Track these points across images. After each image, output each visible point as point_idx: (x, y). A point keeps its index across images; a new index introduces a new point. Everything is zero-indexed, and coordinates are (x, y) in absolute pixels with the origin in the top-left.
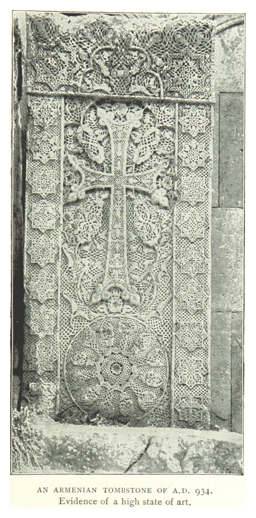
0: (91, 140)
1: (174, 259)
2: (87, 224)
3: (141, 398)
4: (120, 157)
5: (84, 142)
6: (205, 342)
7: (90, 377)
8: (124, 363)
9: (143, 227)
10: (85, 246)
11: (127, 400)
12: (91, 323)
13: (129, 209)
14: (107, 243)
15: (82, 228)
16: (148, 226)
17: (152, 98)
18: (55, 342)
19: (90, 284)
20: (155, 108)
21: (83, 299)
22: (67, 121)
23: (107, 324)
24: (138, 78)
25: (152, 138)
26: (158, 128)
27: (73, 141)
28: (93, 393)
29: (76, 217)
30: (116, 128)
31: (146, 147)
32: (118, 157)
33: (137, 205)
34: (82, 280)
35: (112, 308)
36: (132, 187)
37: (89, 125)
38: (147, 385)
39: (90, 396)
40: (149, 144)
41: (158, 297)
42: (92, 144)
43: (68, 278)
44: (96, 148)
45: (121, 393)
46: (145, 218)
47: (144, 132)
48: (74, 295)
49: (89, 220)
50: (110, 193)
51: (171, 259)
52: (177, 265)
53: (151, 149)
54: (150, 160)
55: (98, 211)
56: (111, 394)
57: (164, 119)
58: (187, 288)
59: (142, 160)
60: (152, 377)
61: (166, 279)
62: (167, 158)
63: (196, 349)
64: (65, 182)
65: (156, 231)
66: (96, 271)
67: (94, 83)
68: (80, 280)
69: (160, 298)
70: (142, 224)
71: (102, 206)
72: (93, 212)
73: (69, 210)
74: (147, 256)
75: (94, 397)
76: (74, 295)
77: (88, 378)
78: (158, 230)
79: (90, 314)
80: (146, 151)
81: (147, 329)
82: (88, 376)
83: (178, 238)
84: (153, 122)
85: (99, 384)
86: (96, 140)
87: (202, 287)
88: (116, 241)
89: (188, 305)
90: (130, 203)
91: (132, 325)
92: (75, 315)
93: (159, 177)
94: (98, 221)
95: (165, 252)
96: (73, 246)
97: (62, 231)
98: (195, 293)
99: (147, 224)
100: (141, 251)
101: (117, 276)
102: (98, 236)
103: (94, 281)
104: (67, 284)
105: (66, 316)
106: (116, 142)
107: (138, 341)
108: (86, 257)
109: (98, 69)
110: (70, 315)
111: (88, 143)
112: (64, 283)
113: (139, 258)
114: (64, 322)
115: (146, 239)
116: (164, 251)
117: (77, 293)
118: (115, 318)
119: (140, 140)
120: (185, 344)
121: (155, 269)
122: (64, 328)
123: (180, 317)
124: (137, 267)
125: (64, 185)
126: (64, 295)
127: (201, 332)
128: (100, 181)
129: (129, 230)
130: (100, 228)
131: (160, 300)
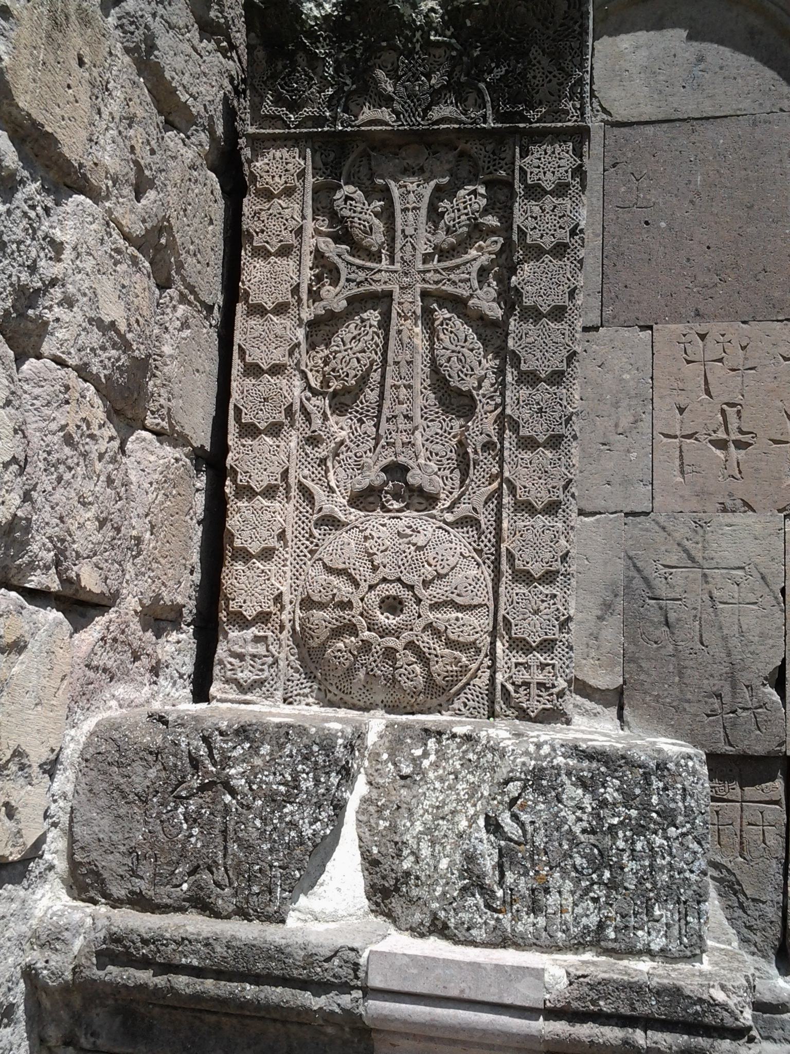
1: (508, 411)
4: (411, 237)
5: (346, 213)
9: (450, 358)
11: (409, 665)
12: (349, 527)
15: (339, 362)
17: (470, 126)
21: (338, 487)
25: (470, 200)
33: (441, 319)
42: (360, 216)
50: (392, 300)
53: (469, 219)
54: (468, 242)
57: (494, 165)
60: (458, 624)
71: (376, 323)
72: (359, 334)
77: (338, 624)
80: (459, 223)
81: (452, 537)
82: (337, 620)
85: (357, 636)
88: (400, 383)
92: (321, 514)
97: (303, 368)
98: (546, 472)
99: (459, 352)
101: (399, 444)
104: (309, 459)
107: (434, 558)
109: (372, 85)
111: (353, 215)
115: (457, 378)
122: (300, 536)
124: (439, 431)
128: (374, 281)
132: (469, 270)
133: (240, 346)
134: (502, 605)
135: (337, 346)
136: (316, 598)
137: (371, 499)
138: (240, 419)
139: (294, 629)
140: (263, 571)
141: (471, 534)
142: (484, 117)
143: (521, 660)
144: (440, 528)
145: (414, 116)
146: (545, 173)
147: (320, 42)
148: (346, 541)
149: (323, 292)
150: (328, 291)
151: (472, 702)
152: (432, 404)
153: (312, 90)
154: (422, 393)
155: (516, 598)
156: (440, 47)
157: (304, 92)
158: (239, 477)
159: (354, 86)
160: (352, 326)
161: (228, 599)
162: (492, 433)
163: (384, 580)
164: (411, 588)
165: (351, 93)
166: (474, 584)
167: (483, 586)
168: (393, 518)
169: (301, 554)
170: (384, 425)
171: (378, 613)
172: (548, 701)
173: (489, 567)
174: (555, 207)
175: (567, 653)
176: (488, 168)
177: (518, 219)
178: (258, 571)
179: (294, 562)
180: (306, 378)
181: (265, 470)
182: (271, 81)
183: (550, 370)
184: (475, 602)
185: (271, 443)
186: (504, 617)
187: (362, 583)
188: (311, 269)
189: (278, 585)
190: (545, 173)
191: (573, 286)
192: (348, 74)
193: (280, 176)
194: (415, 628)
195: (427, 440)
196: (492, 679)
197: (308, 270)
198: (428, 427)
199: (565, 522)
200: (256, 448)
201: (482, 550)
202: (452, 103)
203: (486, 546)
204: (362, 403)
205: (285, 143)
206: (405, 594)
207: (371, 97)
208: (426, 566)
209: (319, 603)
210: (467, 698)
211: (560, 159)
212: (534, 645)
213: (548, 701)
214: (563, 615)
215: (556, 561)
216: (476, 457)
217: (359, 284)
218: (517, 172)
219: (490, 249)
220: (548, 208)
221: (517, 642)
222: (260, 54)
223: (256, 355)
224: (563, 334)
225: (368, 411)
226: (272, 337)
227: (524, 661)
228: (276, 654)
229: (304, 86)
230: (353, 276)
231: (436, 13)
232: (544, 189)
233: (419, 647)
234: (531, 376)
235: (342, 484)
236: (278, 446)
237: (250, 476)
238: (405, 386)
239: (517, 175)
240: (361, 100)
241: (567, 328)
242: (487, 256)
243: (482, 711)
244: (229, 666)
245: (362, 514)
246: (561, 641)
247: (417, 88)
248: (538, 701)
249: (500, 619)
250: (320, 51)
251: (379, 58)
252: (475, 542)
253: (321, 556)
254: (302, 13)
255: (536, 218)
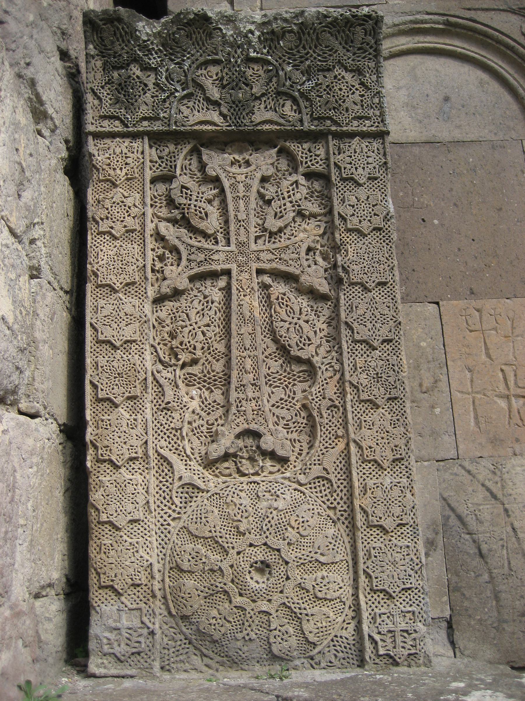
0: (194, 197)
1: (347, 377)
2: (194, 329)
3: (308, 620)
5: (183, 201)
6: (412, 514)
7: (213, 590)
8: (273, 560)
9: (288, 329)
10: (191, 366)
13: (263, 303)
14: (230, 359)
15: (186, 336)
16: (297, 326)
17: (289, 128)
18: (146, 532)
19: (204, 429)
20: (294, 146)
21: (193, 454)
22: (155, 172)
23: (238, 495)
24: (265, 101)
25: (293, 190)
26: (302, 175)
27: (165, 202)
28: (220, 619)
29: (174, 320)
30: (235, 178)
31: (285, 205)
32: (240, 221)
33: (277, 294)
34: (190, 423)
35: (245, 467)
36: (267, 266)
37: (190, 177)
38: (316, 597)
39: (215, 625)
40: (290, 199)
41: (324, 442)
43: (165, 420)
44: (204, 209)
45: (271, 615)
46: (292, 315)
47: (280, 183)
48: (176, 449)
49: (196, 323)
50: (230, 277)
51: (340, 379)
52: (353, 388)
53: (293, 206)
54: (293, 225)
55: (211, 308)
56: (254, 617)
57: (311, 161)
58: (373, 424)
59: (280, 223)
60: (325, 582)
61: (334, 412)
62: (319, 221)
63: (398, 526)
64: (154, 265)
65: (311, 335)
66: (213, 407)
67: (196, 113)
68: (186, 424)
69: (326, 445)
70: (286, 325)
71: (217, 299)
72: (203, 310)
73: (161, 310)
74: (299, 377)
75: (222, 626)
76: (176, 449)
78: (315, 332)
79: (206, 479)
80: (285, 209)
81: (308, 498)
82: (209, 589)
83: (350, 342)
84: (293, 168)
85: (230, 602)
86: (202, 198)
87: (398, 420)
88: (245, 354)
89: (377, 452)
90: (265, 294)
91: (282, 493)
92: (181, 483)
93: (309, 250)
94: (212, 323)
95: (330, 367)
96: (171, 366)
97: (152, 342)
98: (388, 432)
99: (296, 324)
100: (288, 369)
102: (214, 348)
103: (210, 422)
104: (165, 430)
105: (164, 485)
106: (236, 199)
107: (296, 520)
108: (194, 385)
110: (171, 484)
111: (189, 202)
112: (158, 429)
113: (285, 381)
114: (160, 496)
115: (296, 348)
116: (327, 366)
117: (181, 445)
118: (251, 483)
119: (274, 195)
120: (378, 519)
121: (314, 397)
122: (162, 506)
123: (364, 474)
124: (283, 396)
125: (153, 271)
126: (159, 449)
127: (405, 496)
129: (265, 337)
130: (215, 335)
131: (327, 448)
132: (298, 250)
133: (91, 325)
134: (361, 561)
135: (184, 321)
136: (185, 566)
137: (226, 464)
138: (97, 394)
139: (165, 597)
140: (130, 543)
141: (324, 493)
142: (301, 121)
143: (383, 610)
144: (295, 490)
145: (239, 118)
146: (356, 168)
147: (152, 55)
148: (209, 508)
149: (167, 273)
150: (171, 271)
151: (341, 654)
152: (275, 371)
153: (147, 95)
154: (264, 361)
155: (373, 552)
156: (257, 62)
157: (140, 96)
158: (100, 451)
159: (185, 92)
160: (196, 302)
161: (98, 574)
162: (334, 397)
163: (251, 545)
164: (279, 550)
165: (183, 98)
166: (333, 541)
167: (341, 543)
168: (251, 483)
169: (165, 523)
170: (234, 395)
171: (248, 577)
172: (411, 645)
173: (343, 523)
174: (368, 197)
175: (423, 599)
176: (306, 163)
177: (338, 208)
178: (127, 544)
179: (158, 531)
180: (156, 351)
181: (125, 443)
182: (109, 86)
183: (381, 339)
184: (337, 560)
185: (129, 417)
186: (364, 570)
187: (231, 551)
188: (153, 250)
189: (146, 557)
190: (356, 168)
191: (392, 265)
192: (178, 82)
193: (121, 169)
194: (285, 591)
195: (273, 406)
196: (358, 629)
197: (151, 252)
198: (273, 393)
199: (408, 477)
200: (114, 422)
201: (335, 508)
202: (271, 108)
203: (338, 503)
204: (209, 373)
205: (123, 140)
206: (271, 558)
207: (199, 101)
208: (290, 529)
209: (189, 572)
210: (335, 650)
211: (368, 157)
212: (394, 595)
213: (411, 645)
214: (417, 564)
215: (406, 514)
216: (322, 420)
217: (200, 264)
218: (332, 166)
219: (315, 232)
220: (363, 197)
221: (378, 593)
222: (99, 63)
223: (107, 333)
224: (389, 307)
225: (215, 380)
226: (122, 314)
227: (387, 611)
228: (150, 625)
229: (139, 92)
230: (192, 257)
231: (253, 35)
232: (356, 182)
233: (289, 608)
234: (364, 345)
235: (197, 451)
236: (135, 420)
237: (111, 450)
238: (249, 357)
239: (333, 170)
240: (191, 104)
241: (391, 301)
242: (313, 238)
243: (351, 661)
244: (105, 641)
245: (220, 480)
246: (416, 588)
247: (241, 95)
248: (403, 647)
249: (361, 572)
250: (153, 62)
251: (205, 69)
252: (328, 500)
253: (186, 525)
254: (136, 30)
255: (353, 206)
